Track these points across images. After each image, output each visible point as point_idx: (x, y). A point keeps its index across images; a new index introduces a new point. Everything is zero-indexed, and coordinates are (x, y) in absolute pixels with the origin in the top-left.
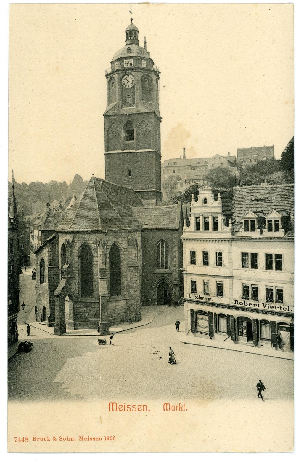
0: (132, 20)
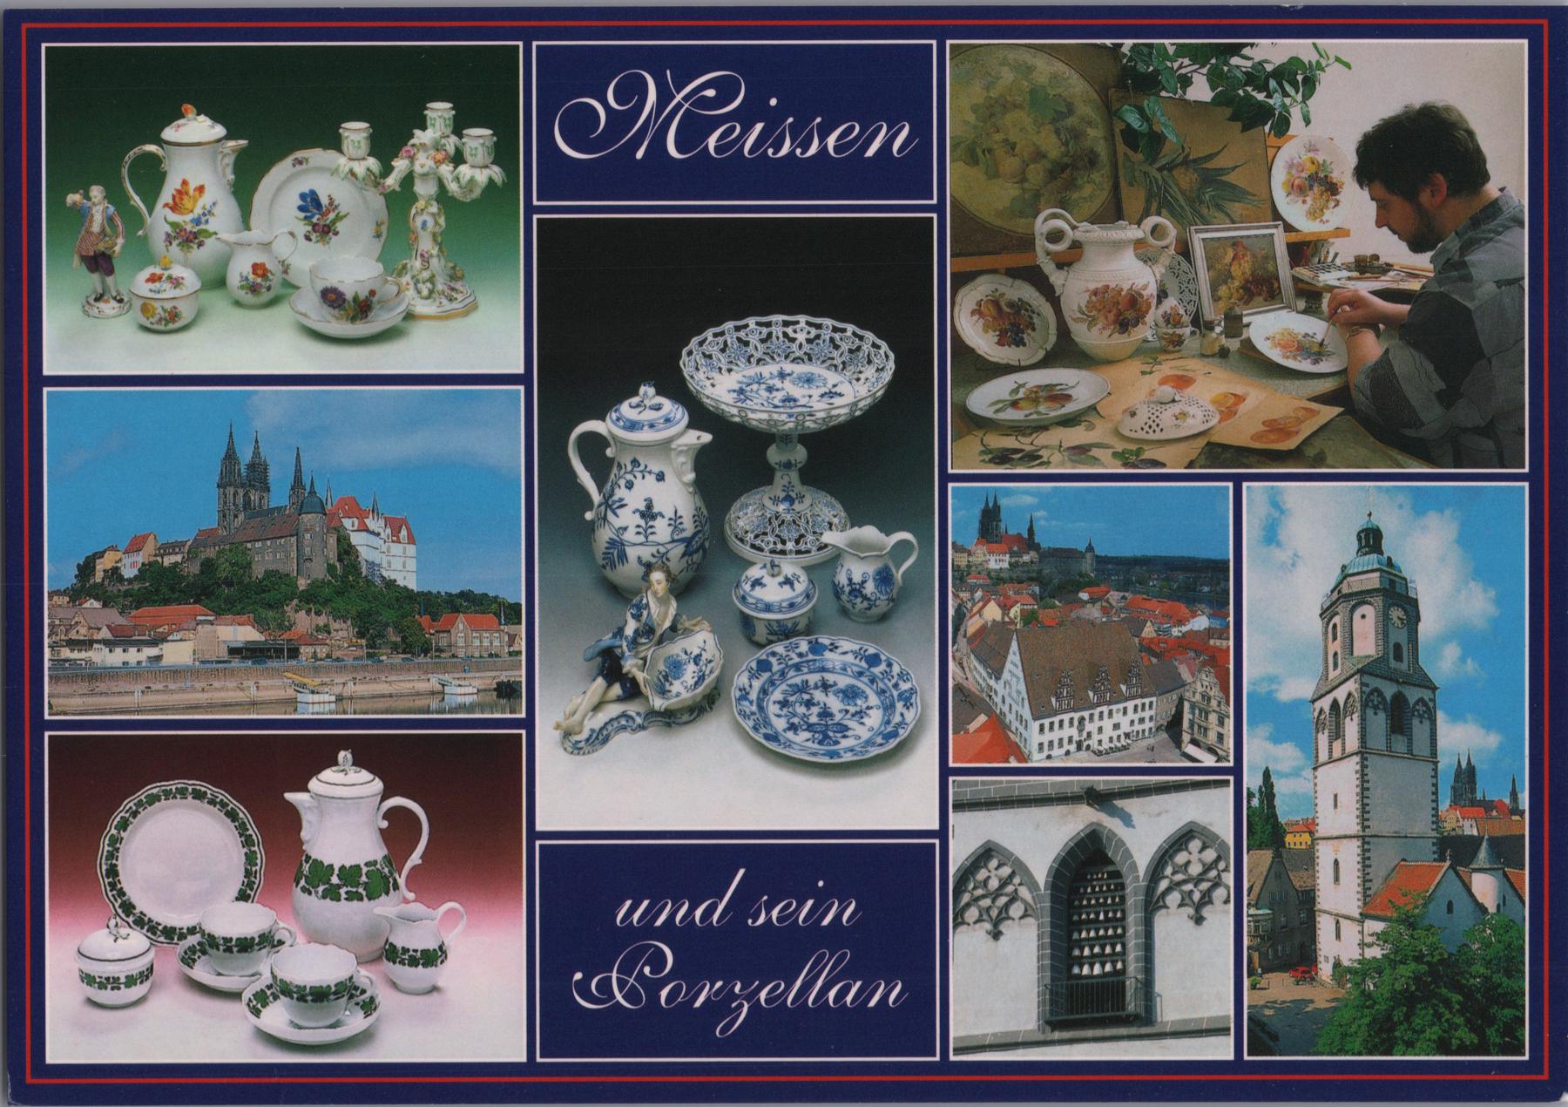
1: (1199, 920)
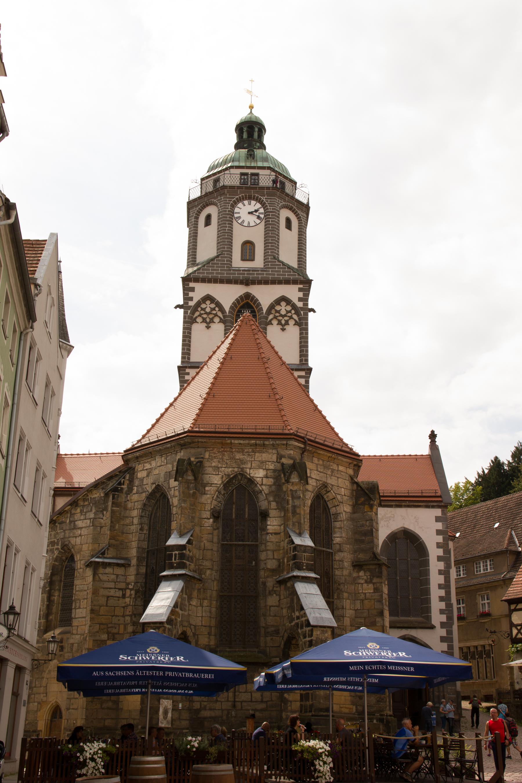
0: (251, 107)
1: (283, 330)
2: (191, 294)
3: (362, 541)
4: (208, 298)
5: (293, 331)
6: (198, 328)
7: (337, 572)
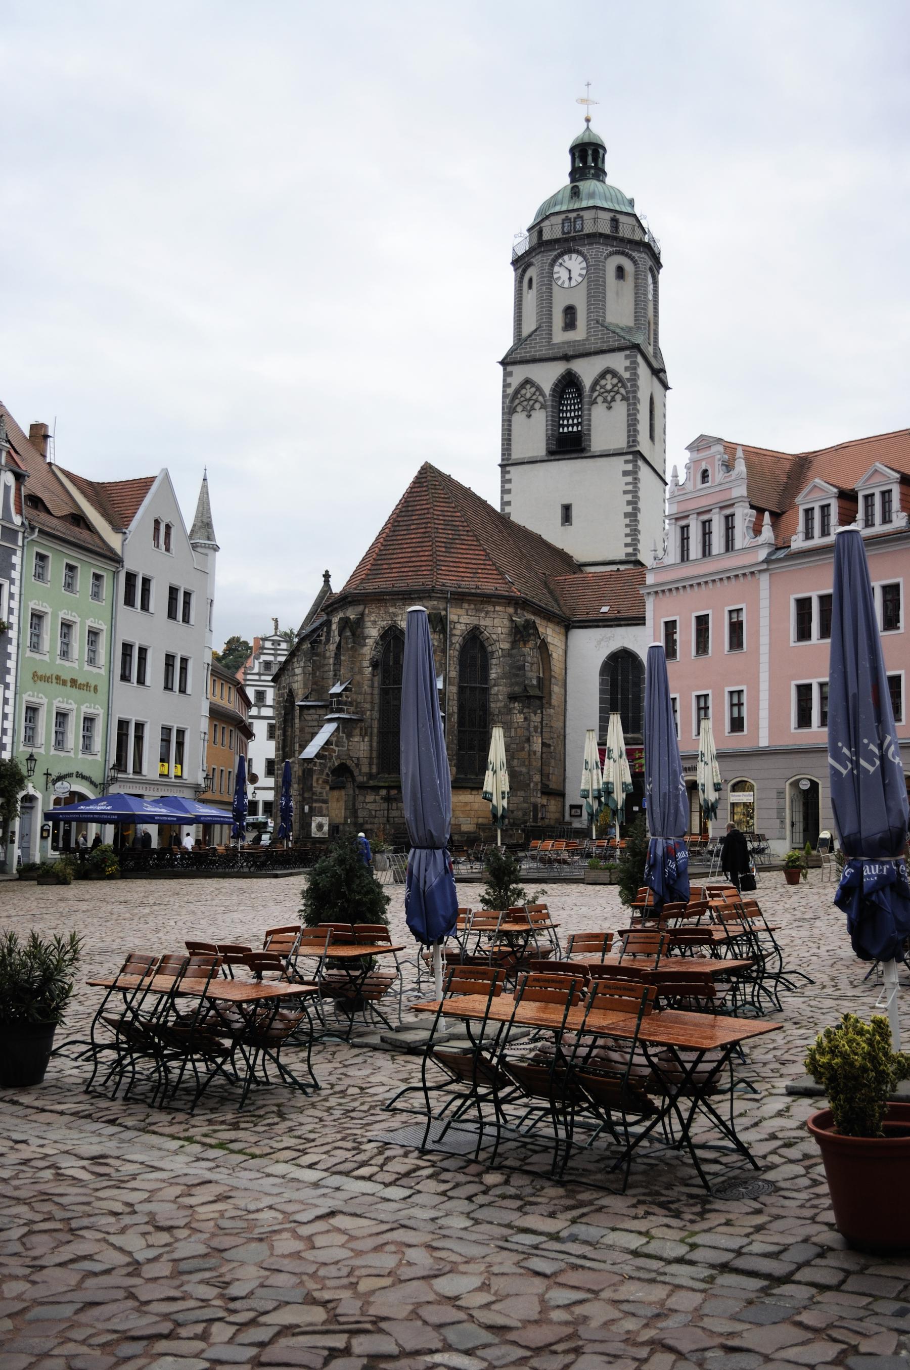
2: (509, 380)
3: (517, 675)
4: (527, 382)
5: (620, 408)
6: (519, 419)
7: (492, 705)
